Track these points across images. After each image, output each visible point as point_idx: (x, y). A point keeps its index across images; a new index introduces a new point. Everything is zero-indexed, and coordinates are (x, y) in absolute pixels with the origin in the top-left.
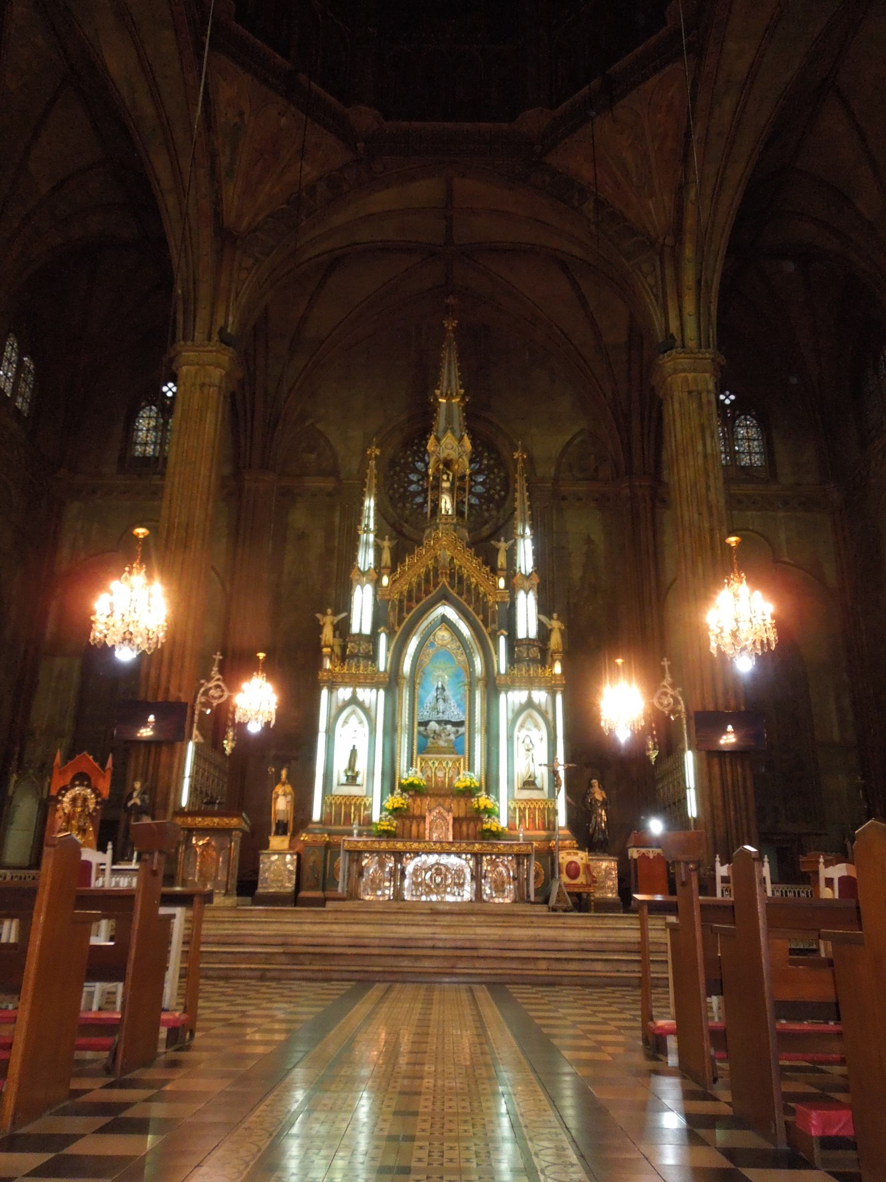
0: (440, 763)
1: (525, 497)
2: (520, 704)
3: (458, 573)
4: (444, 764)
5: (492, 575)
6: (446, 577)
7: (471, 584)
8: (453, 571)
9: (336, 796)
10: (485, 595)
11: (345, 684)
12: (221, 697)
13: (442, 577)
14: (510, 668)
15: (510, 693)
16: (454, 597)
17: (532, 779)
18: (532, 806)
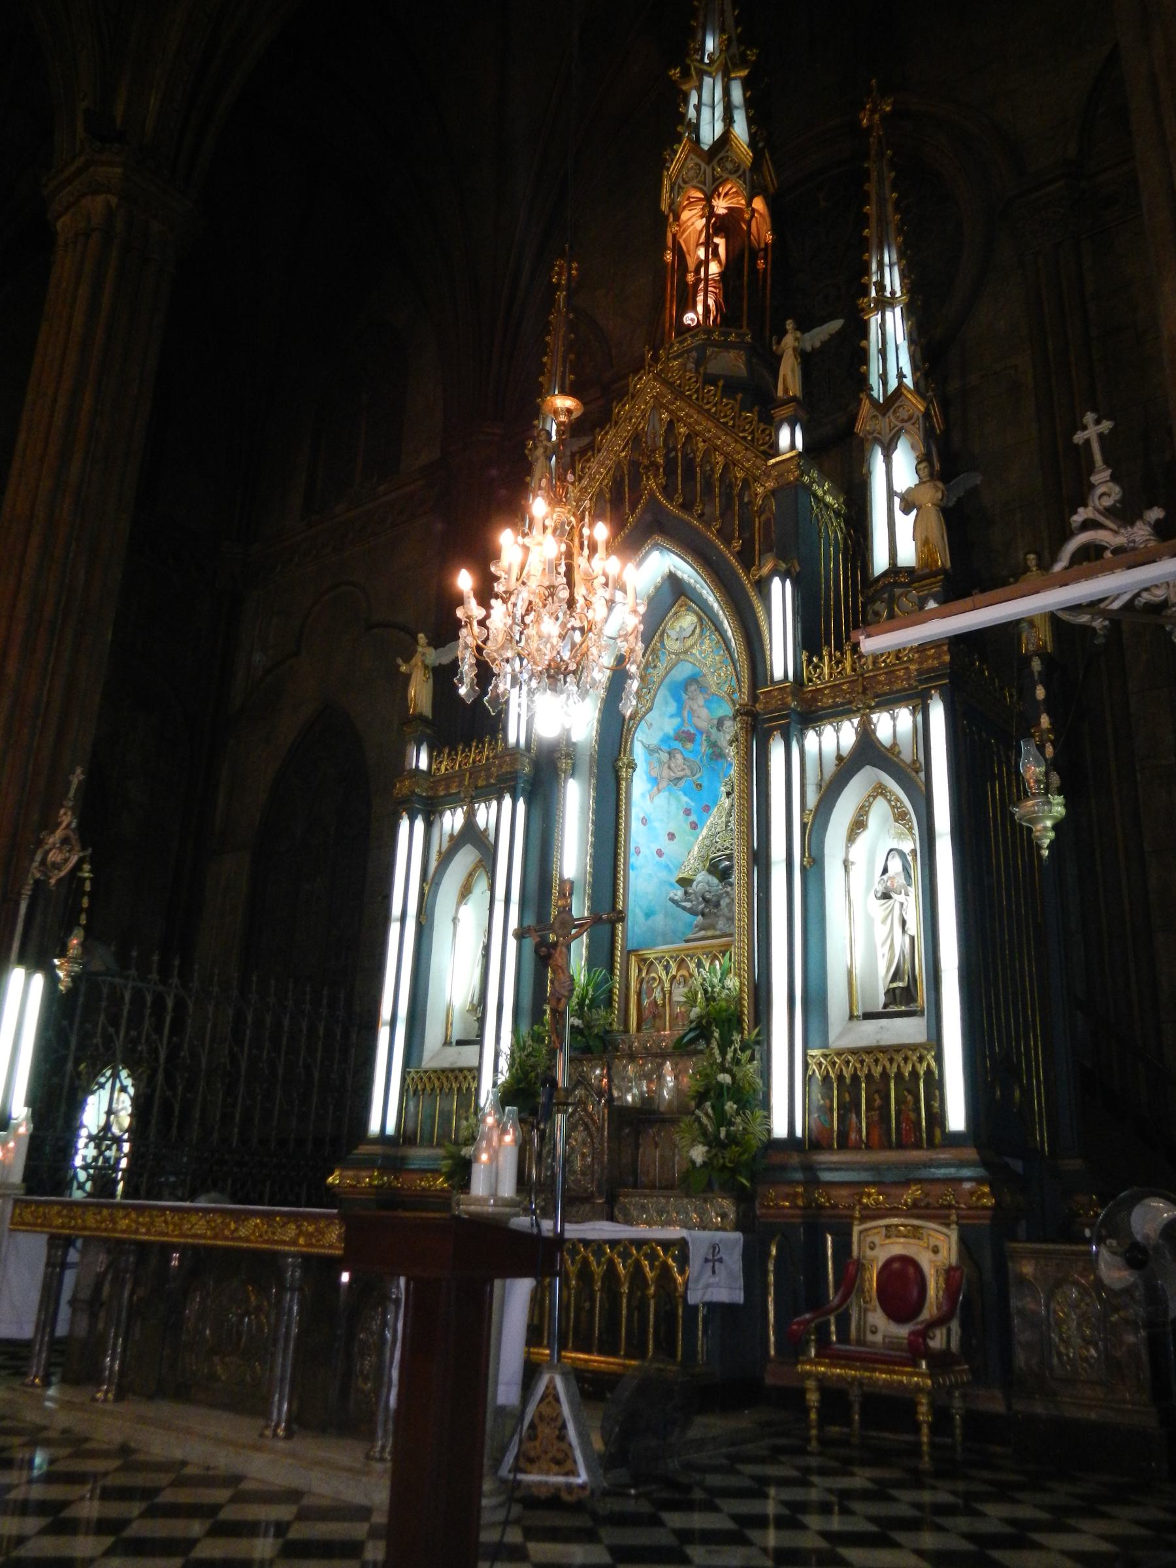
0: (681, 964)
1: (890, 208)
2: (839, 758)
3: (685, 455)
4: (692, 966)
5: (762, 426)
6: (656, 476)
7: (713, 471)
8: (673, 454)
9: (426, 1072)
10: (746, 483)
11: (452, 801)
12: (66, 860)
13: (648, 478)
14: (810, 661)
15: (811, 735)
16: (676, 517)
17: (901, 984)
18: (877, 1071)
